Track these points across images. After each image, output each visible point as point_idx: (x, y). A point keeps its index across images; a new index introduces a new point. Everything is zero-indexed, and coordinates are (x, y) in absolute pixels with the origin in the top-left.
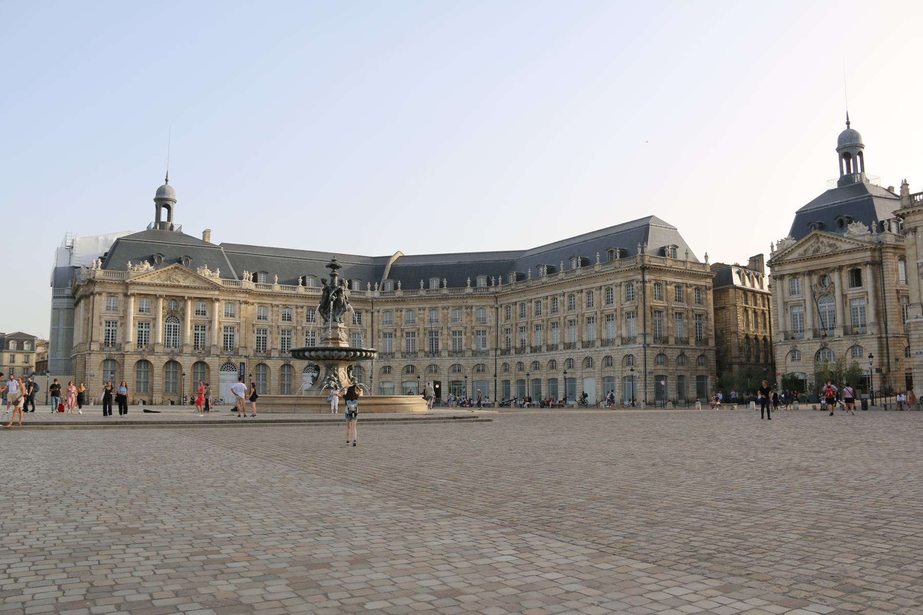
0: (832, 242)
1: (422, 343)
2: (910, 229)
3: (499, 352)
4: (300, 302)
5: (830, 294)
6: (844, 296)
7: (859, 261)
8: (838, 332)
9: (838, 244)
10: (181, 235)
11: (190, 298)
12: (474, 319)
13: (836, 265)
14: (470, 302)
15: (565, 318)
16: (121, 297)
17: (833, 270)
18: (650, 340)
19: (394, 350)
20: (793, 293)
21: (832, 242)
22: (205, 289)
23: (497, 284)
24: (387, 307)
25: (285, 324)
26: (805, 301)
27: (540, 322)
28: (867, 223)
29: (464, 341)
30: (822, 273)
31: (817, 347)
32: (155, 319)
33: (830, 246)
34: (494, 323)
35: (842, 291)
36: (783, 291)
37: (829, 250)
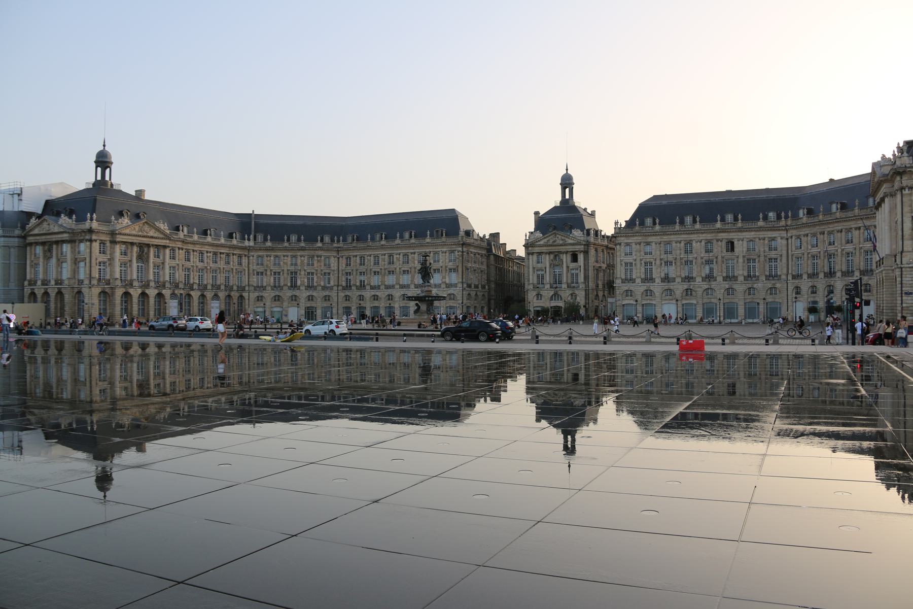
1: (285, 280)
3: (340, 288)
4: (210, 249)
5: (560, 265)
6: (568, 267)
8: (564, 286)
10: (120, 192)
11: (153, 245)
12: (322, 264)
14: (320, 253)
16: (108, 244)
18: (465, 285)
19: (265, 284)
22: (162, 239)
23: (338, 241)
24: (260, 253)
25: (200, 265)
28: (582, 231)
29: (315, 279)
31: (552, 293)
32: (131, 261)
34: (336, 268)
37: (561, 242)
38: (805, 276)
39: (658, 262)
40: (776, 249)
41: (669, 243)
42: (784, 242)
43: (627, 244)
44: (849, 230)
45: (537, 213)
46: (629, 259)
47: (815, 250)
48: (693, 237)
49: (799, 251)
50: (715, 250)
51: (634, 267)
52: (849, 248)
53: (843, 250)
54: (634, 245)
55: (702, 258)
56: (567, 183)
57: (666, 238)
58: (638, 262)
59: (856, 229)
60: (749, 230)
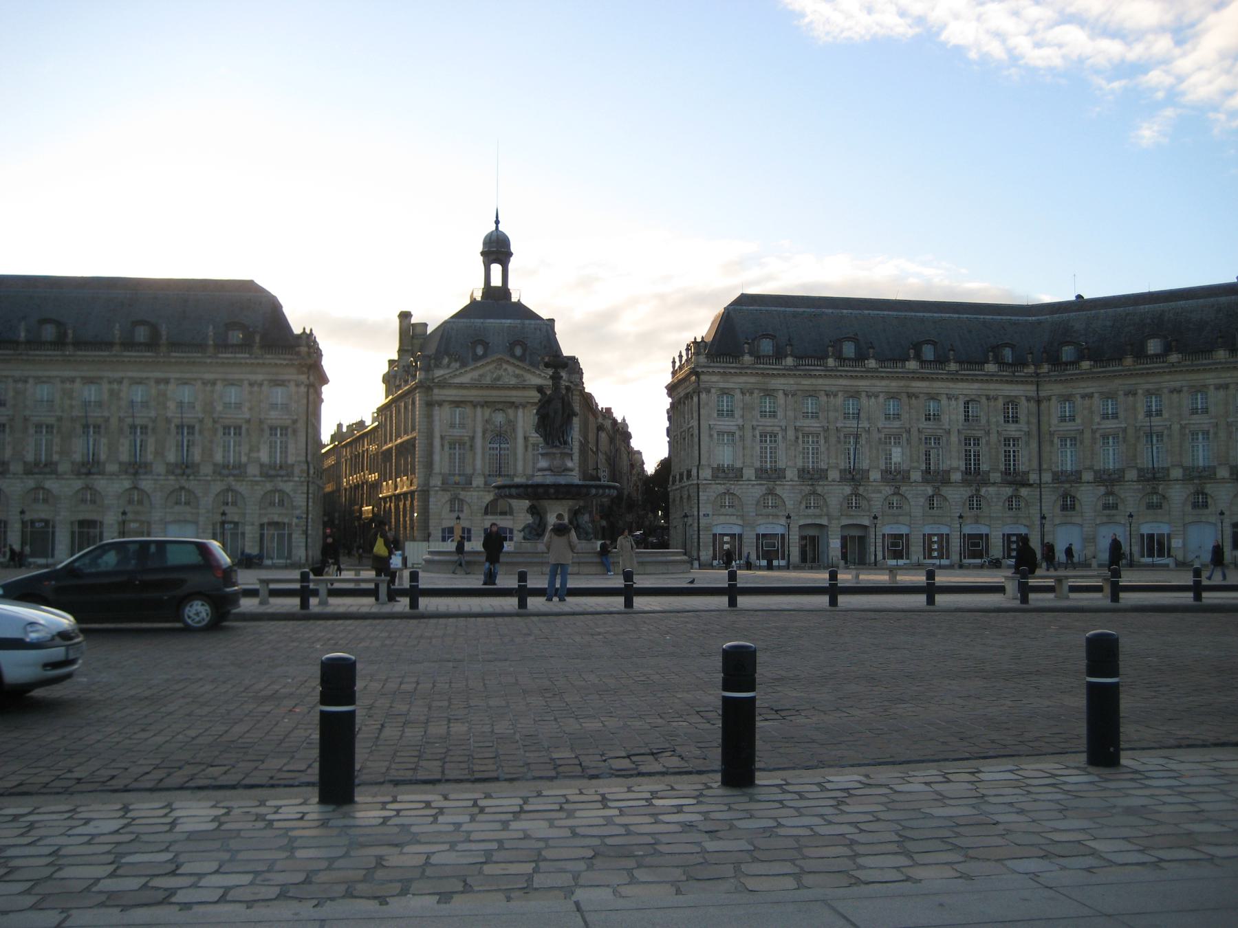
0: (518, 371)
2: (705, 389)
15: (121, 420)
20: (452, 426)
26: (473, 438)
27: (51, 421)
33: (517, 376)
35: (525, 432)
37: (513, 381)
39: (791, 434)
40: (1016, 420)
42: (1033, 405)
43: (724, 392)
44: (1202, 389)
45: (405, 316)
47: (1110, 425)
48: (862, 384)
49: (1069, 426)
52: (1201, 421)
53: (1183, 427)
54: (738, 396)
56: (497, 250)
58: (748, 434)
59: (1218, 387)
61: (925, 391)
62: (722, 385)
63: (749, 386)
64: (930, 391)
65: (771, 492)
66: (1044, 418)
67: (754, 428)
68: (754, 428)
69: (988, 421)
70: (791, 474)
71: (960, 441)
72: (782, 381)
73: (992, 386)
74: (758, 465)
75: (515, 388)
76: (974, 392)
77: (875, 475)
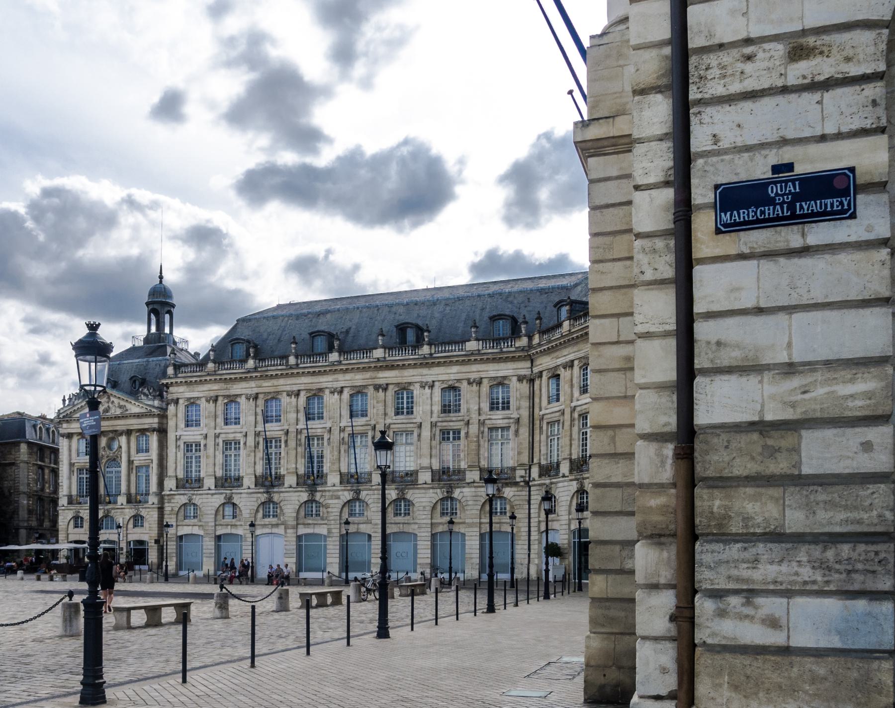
0: (122, 403)
2: (172, 400)
7: (146, 427)
9: (128, 406)
13: (124, 428)
17: (121, 434)
21: (122, 403)
30: (111, 435)
33: (120, 407)
35: (129, 456)
36: (70, 451)
37: (118, 412)
38: (565, 468)
41: (274, 397)
42: (525, 387)
46: (192, 435)
50: (371, 411)
51: (202, 453)
54: (203, 403)
55: (342, 430)
57: (267, 386)
58: (211, 442)
60: (448, 362)
61: (395, 381)
62: (189, 395)
63: (212, 394)
64: (399, 380)
65: (229, 501)
66: (537, 400)
67: (217, 436)
68: (217, 436)
69: (468, 410)
70: (249, 481)
71: (433, 438)
72: (244, 384)
73: (475, 367)
74: (219, 473)
75: (117, 418)
76: (452, 377)
77: (333, 479)
